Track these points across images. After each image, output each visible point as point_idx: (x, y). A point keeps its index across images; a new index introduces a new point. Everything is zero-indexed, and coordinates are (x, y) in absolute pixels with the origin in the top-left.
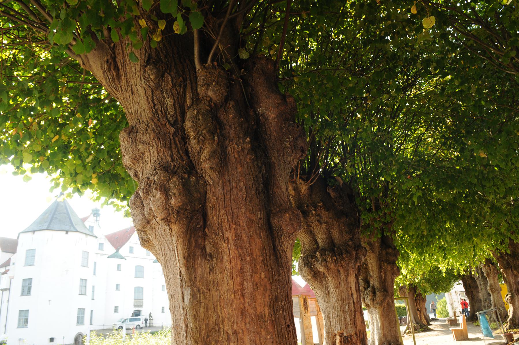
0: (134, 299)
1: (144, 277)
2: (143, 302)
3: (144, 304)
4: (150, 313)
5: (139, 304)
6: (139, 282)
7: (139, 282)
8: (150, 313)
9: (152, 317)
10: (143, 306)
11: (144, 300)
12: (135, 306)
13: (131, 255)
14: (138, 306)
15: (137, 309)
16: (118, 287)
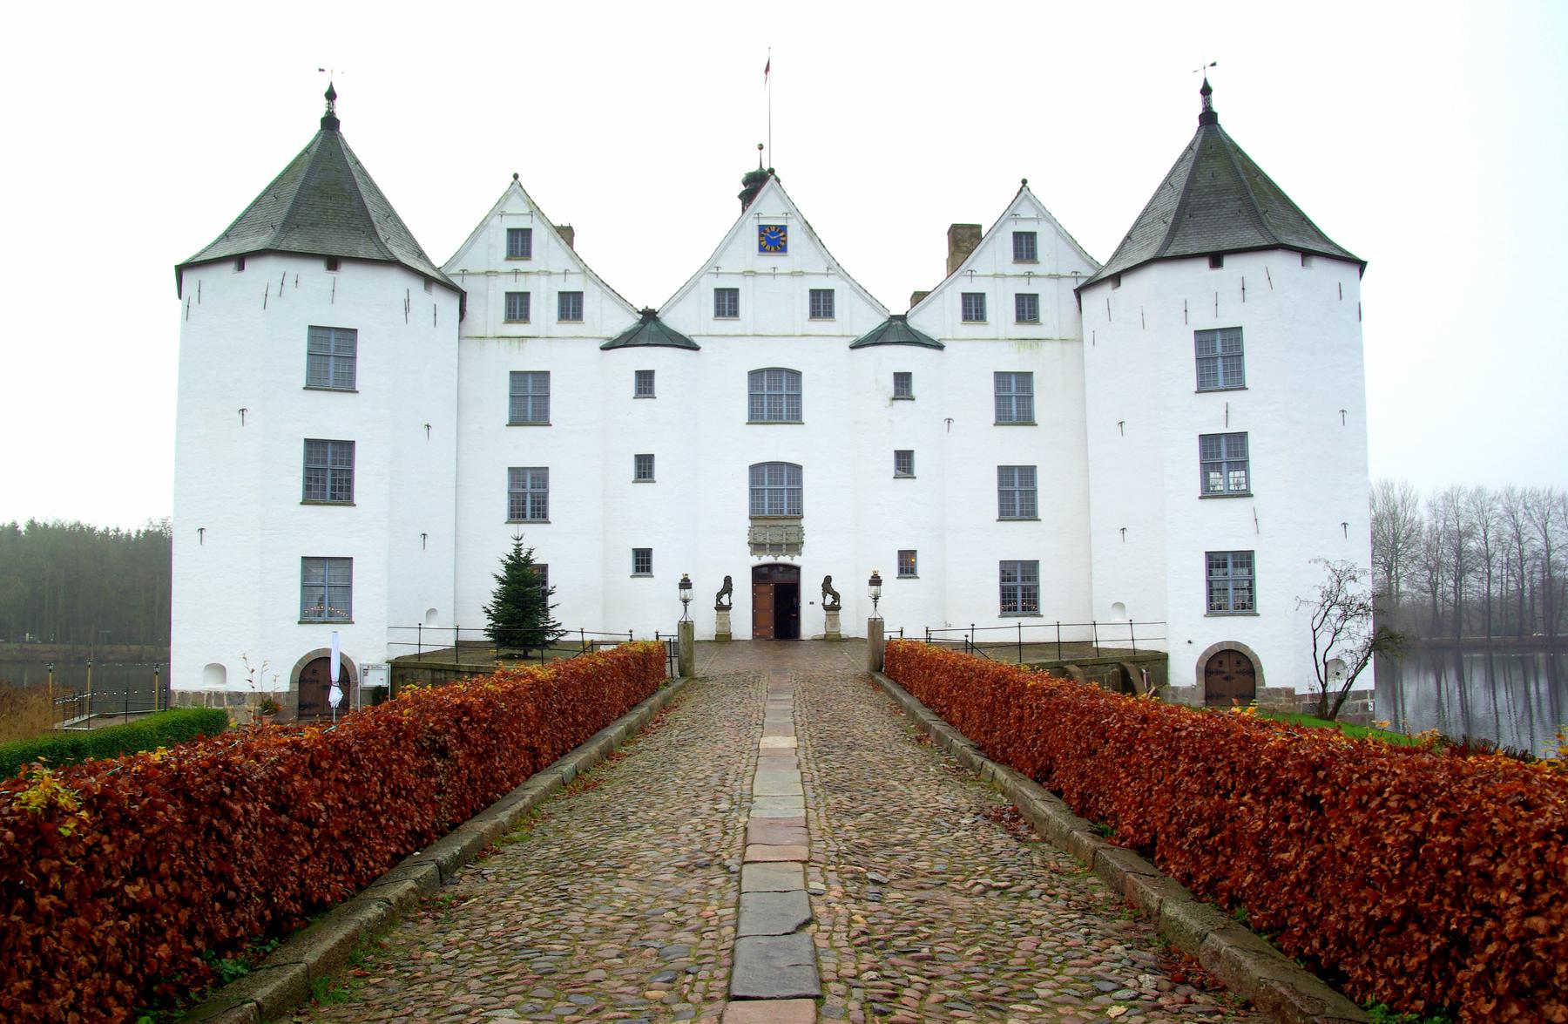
0: (751, 518)
1: (1037, 419)
2: (800, 529)
3: (805, 539)
4: (828, 580)
5: (776, 540)
6: (776, 443)
7: (776, 443)
8: (828, 580)
9: (836, 596)
10: (804, 550)
11: (804, 523)
12: (757, 547)
13: (727, 326)
14: (776, 548)
15: (768, 559)
16: (644, 467)
